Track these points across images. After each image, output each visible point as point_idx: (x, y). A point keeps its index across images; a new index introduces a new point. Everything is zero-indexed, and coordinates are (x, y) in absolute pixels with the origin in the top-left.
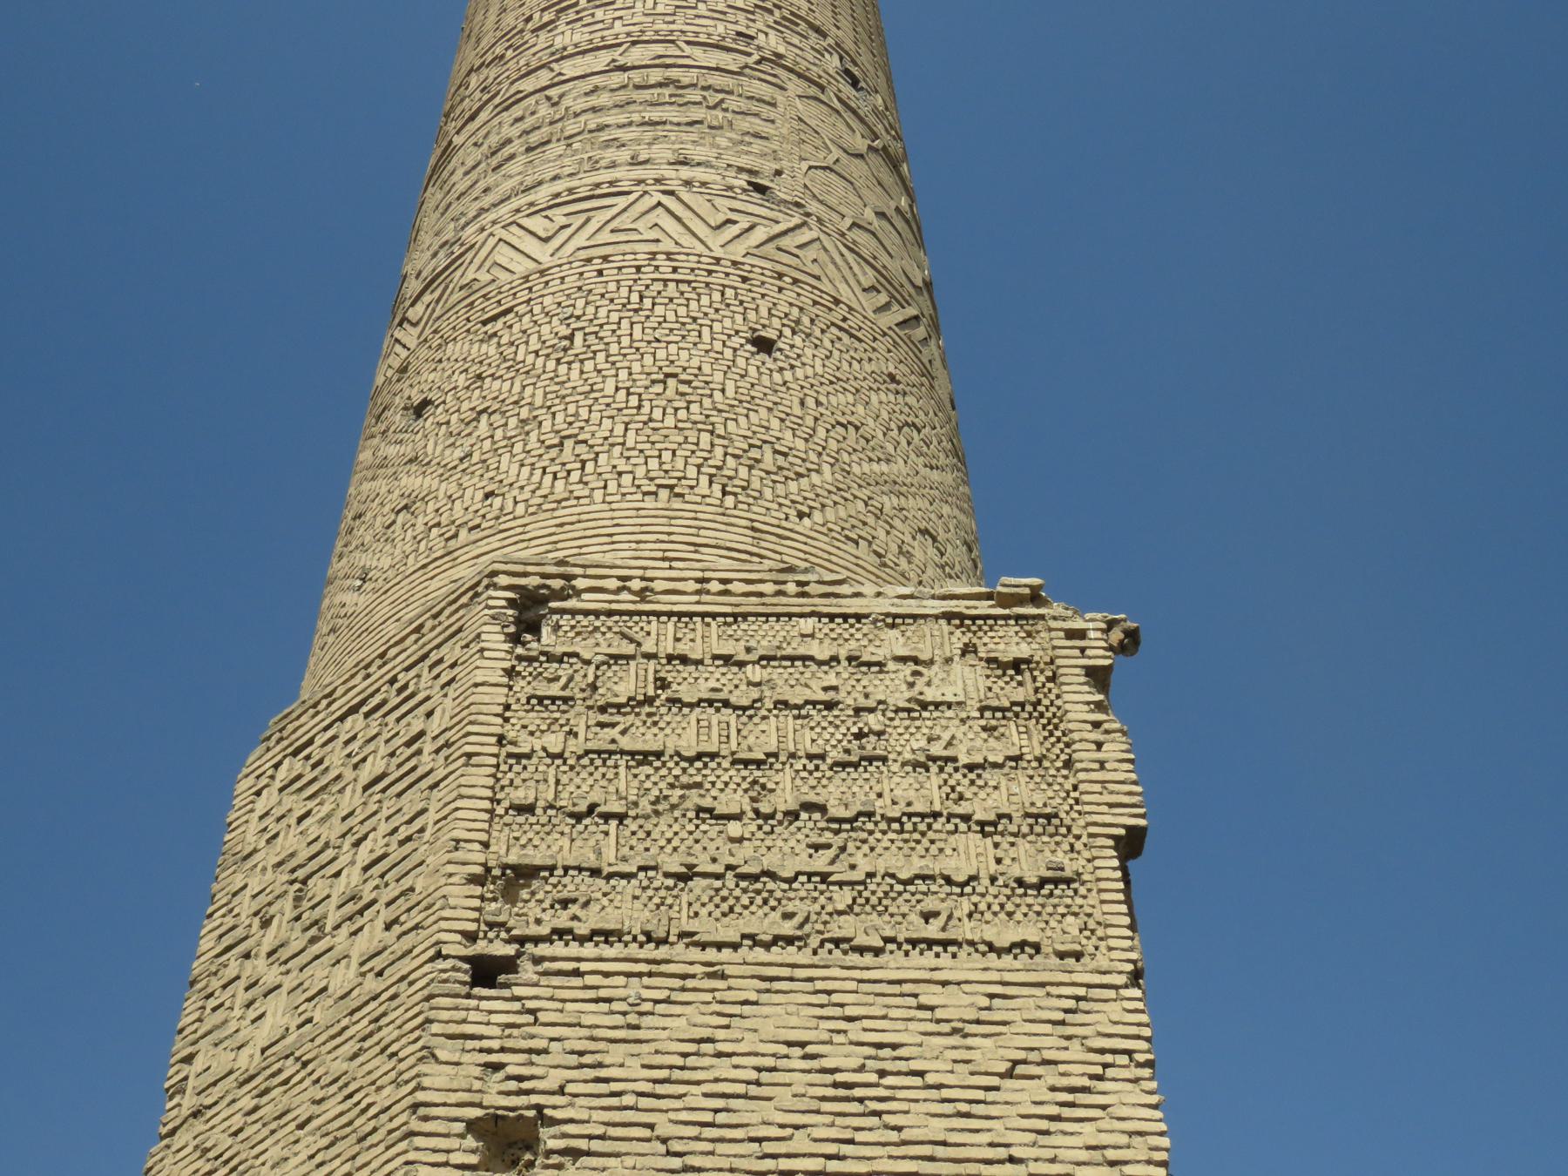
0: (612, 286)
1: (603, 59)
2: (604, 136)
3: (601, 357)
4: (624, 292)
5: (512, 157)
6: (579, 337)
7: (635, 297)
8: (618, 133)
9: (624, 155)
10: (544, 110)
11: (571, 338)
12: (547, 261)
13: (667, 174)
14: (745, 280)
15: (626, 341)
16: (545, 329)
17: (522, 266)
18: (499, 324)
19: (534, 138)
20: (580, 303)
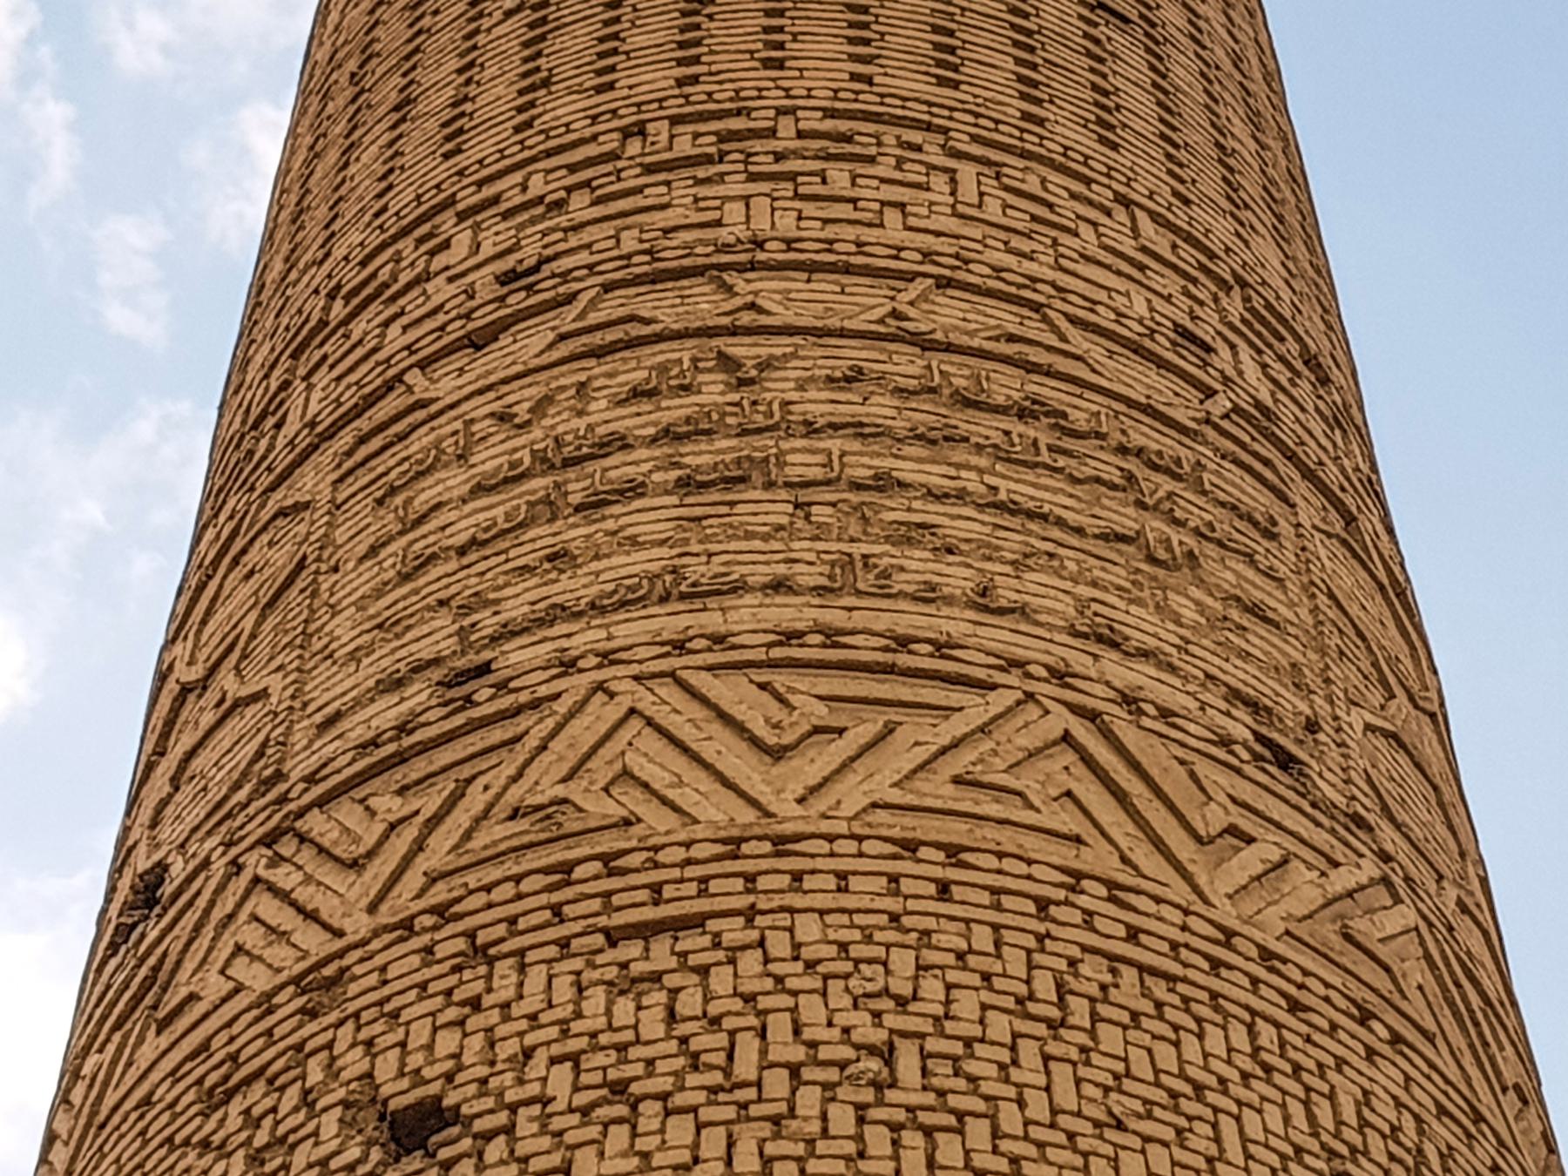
0: (983, 938)
1: (866, 304)
2: (894, 510)
3: (978, 1131)
4: (1015, 962)
5: (634, 489)
6: (908, 1062)
7: (1044, 986)
8: (932, 513)
9: (958, 578)
10: (713, 391)
11: (887, 1054)
12: (790, 815)
13: (1080, 662)
14: (1295, 1007)
15: (1038, 1107)
16: (812, 1010)
17: (716, 811)
18: (661, 954)
19: (699, 456)
20: (903, 962)
